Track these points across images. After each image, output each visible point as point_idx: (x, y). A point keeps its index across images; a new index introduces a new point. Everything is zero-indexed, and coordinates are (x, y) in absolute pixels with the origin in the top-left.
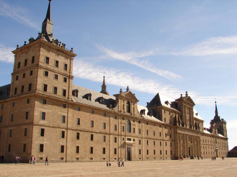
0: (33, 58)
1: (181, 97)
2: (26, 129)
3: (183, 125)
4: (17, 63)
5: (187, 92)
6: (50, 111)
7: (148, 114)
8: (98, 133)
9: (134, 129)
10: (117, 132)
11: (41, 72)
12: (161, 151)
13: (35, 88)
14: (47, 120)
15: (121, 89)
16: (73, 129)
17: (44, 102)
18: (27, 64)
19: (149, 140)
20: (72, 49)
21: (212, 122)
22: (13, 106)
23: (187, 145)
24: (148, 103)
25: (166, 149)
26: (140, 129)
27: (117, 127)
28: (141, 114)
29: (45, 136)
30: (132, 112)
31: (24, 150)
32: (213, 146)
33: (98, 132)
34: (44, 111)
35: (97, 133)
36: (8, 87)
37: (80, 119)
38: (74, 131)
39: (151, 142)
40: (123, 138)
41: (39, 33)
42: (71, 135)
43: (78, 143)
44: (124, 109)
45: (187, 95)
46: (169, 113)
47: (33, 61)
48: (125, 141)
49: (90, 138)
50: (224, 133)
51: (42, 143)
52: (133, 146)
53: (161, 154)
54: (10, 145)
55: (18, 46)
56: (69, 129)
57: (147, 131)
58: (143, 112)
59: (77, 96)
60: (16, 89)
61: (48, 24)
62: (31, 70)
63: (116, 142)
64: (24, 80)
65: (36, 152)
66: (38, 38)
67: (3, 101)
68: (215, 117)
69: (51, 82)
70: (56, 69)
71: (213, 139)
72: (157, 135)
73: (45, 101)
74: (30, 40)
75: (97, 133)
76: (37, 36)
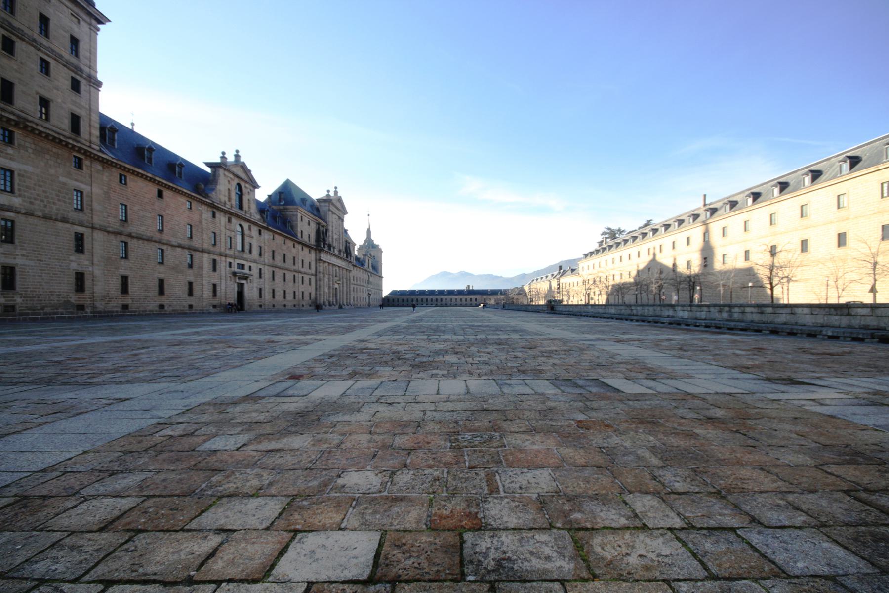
1: (328, 195)
5: (336, 188)
6: (30, 169)
8: (175, 246)
14: (20, 196)
16: (110, 229)
17: (4, 135)
29: (17, 241)
35: (172, 246)
38: (112, 237)
39: (279, 274)
44: (230, 199)
45: (336, 192)
46: (307, 220)
48: (232, 269)
56: (96, 229)
57: (273, 251)
63: (214, 270)
68: (366, 241)
70: (43, 41)
75: (172, 246)
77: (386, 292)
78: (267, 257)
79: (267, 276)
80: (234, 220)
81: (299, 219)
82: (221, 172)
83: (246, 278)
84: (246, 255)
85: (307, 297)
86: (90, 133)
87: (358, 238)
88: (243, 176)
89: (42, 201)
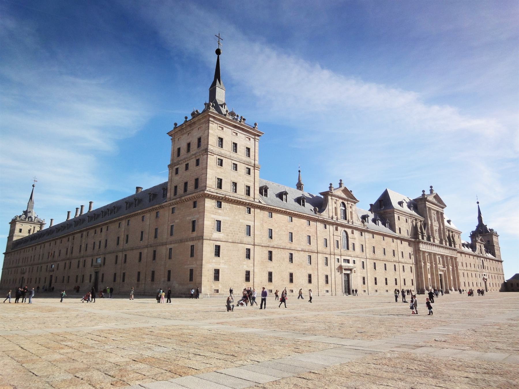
0: (199, 140)
1: (424, 195)
2: (192, 246)
3: (429, 239)
4: (176, 149)
5: (431, 187)
6: (227, 218)
7: (374, 221)
10: (327, 250)
11: (212, 161)
12: (396, 280)
13: (203, 185)
15: (331, 184)
16: (263, 245)
18: (191, 150)
19: (377, 263)
20: (255, 124)
21: (473, 235)
22: (172, 213)
23: (437, 271)
24: (371, 205)
25: (404, 277)
27: (328, 242)
28: (363, 222)
30: (350, 219)
31: (191, 279)
32: (478, 273)
33: (300, 249)
36: (164, 187)
37: (272, 230)
38: (264, 249)
40: (338, 259)
41: (205, 104)
42: (259, 254)
43: (271, 266)
44: (336, 214)
45: (431, 191)
46: (405, 218)
47: (199, 145)
48: (340, 263)
49: (288, 259)
50: (496, 251)
51: (217, 267)
52: (353, 271)
53: (396, 284)
54: (169, 272)
55: (176, 124)
57: (374, 247)
58: (364, 218)
59: (266, 195)
60: (176, 187)
61: (218, 89)
62: (197, 158)
63: (327, 264)
64: (188, 173)
65: (208, 281)
66: (204, 111)
67: (157, 206)
68: (478, 227)
69: (228, 175)
70: (233, 155)
71: (478, 261)
72: (389, 254)
73: (219, 203)
74: (193, 114)
76: (204, 107)
77: (508, 276)
78: (369, 251)
79: (368, 267)
80: (339, 228)
82: (329, 197)
89: (232, 234)
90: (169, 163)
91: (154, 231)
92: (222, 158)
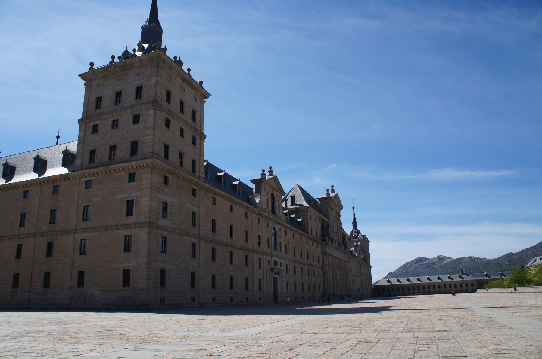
5: (332, 186)
9: (280, 243)
15: (263, 171)
16: (208, 239)
18: (122, 101)
22: (86, 188)
23: (336, 276)
26: (286, 245)
33: (239, 247)
34: (167, 199)
40: (269, 260)
54: (81, 274)
55: (92, 64)
57: (294, 248)
60: (93, 152)
63: (260, 267)
78: (291, 252)
81: (309, 218)
83: (278, 274)
84: (278, 253)
85: (317, 289)
86: (200, 171)
87: (348, 229)
88: (275, 186)
90: (80, 117)
91: (49, 213)
92: (170, 118)
